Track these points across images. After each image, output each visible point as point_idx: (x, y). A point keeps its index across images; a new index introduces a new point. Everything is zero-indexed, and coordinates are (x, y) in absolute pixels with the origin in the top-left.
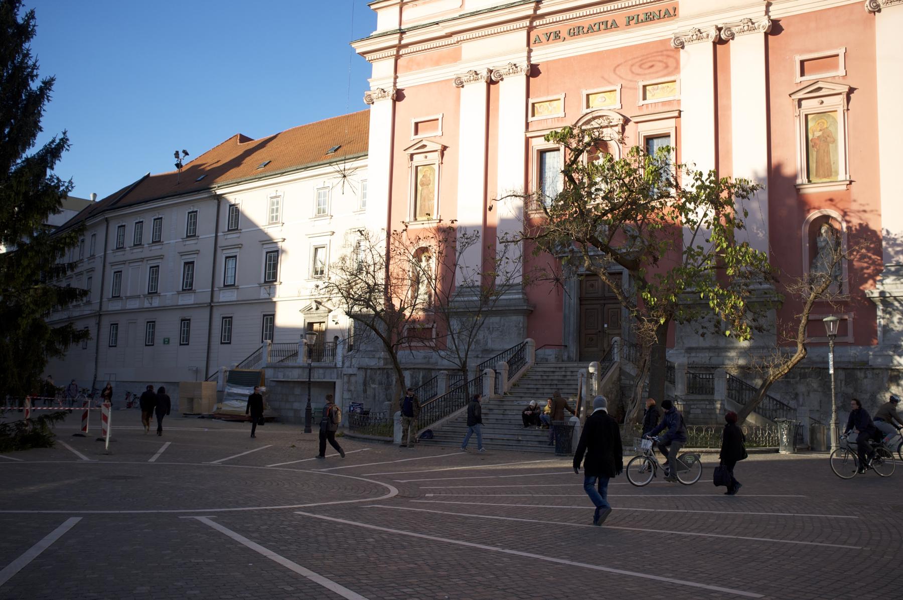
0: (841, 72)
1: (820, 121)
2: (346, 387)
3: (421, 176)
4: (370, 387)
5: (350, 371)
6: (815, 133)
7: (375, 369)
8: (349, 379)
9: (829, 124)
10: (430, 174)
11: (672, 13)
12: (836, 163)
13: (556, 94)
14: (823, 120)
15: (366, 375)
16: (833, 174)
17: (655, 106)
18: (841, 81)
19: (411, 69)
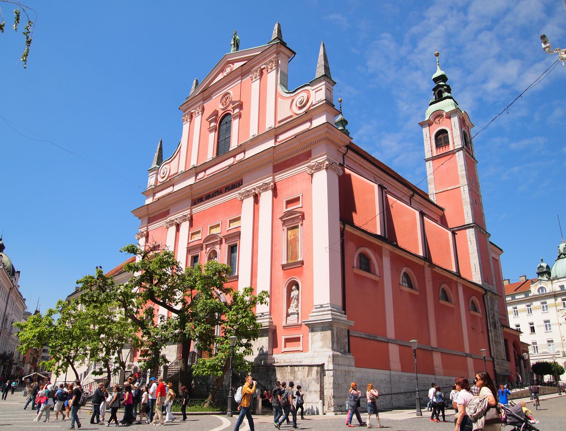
11: (241, 184)
12: (298, 252)
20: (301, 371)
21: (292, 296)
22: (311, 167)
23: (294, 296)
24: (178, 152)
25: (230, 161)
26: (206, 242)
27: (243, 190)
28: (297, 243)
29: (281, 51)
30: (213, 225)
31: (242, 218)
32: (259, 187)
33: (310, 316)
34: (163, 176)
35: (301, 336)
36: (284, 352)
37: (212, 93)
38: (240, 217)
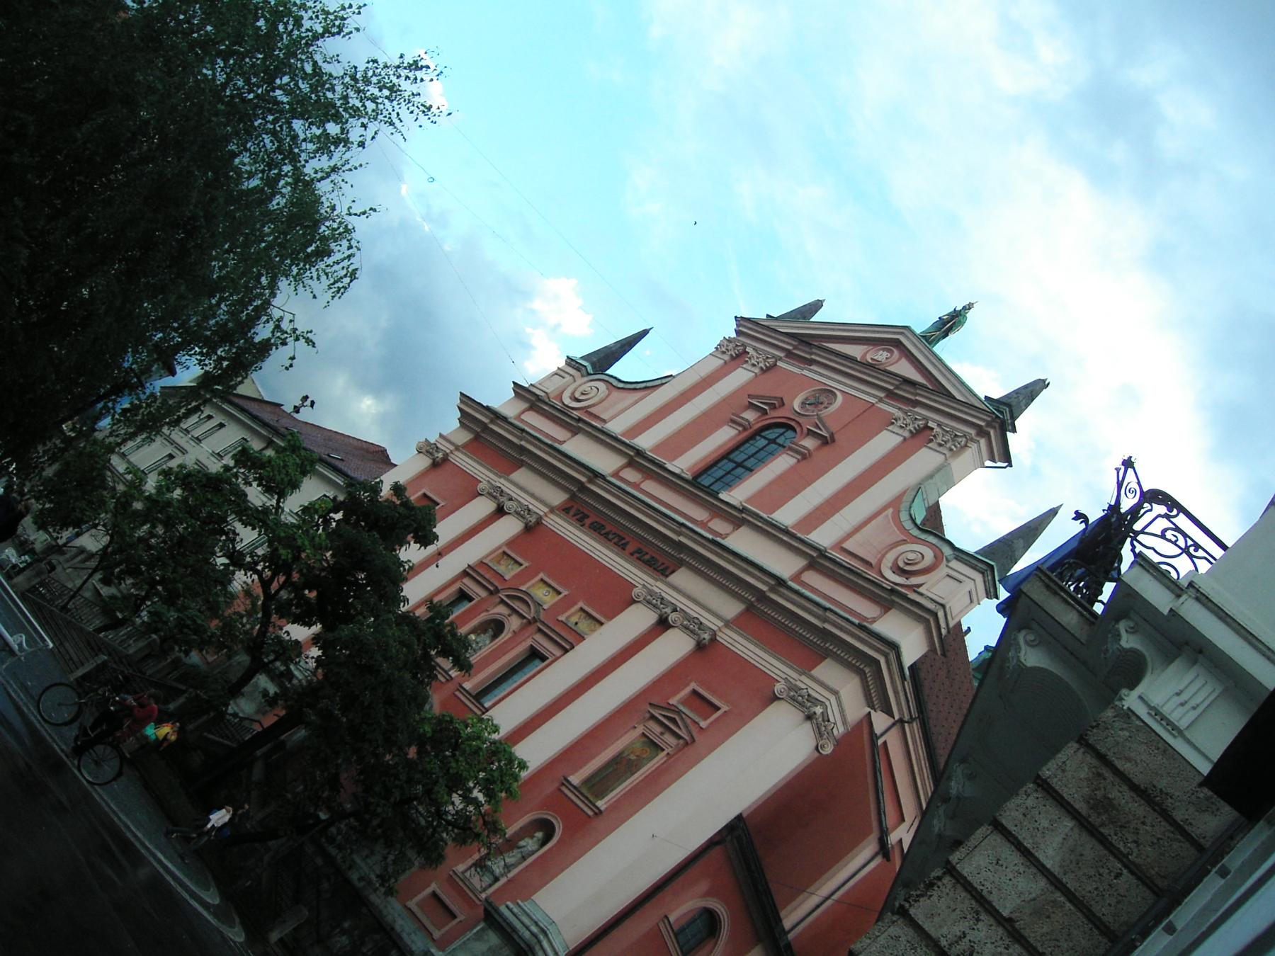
11: (667, 573)
13: (526, 559)
14: (648, 750)
21: (522, 843)
22: (792, 688)
23: (524, 847)
24: (646, 388)
25: (699, 514)
26: (507, 596)
27: (659, 587)
29: (987, 435)
31: (604, 626)
33: (507, 907)
34: (577, 395)
35: (461, 917)
36: (410, 909)
37: (812, 362)
38: (602, 624)
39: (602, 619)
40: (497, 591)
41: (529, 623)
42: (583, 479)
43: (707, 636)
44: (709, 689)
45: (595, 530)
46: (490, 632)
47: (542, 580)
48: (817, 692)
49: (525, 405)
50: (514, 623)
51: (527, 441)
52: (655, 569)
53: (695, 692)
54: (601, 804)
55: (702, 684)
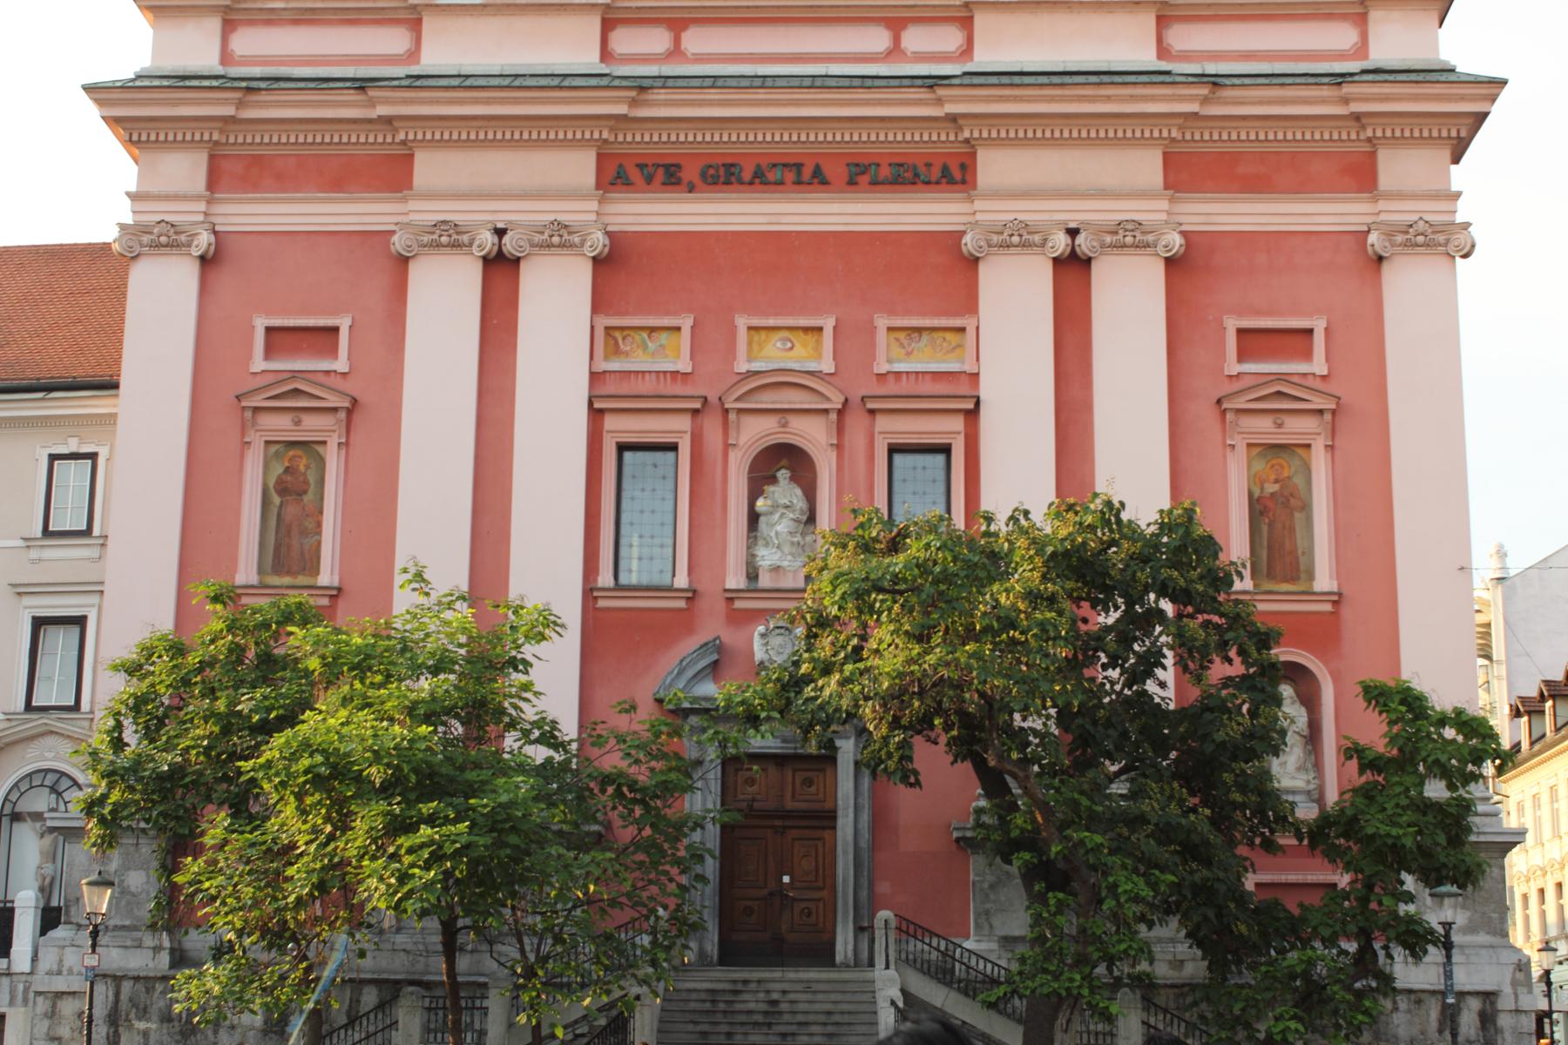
0: (1318, 365)
1: (1274, 462)
2: (43, 1027)
3: (280, 470)
4: (131, 1027)
5: (60, 984)
6: (1266, 485)
7: (146, 978)
8: (54, 1006)
9: (1293, 470)
10: (307, 467)
11: (957, 174)
13: (676, 313)
14: (1280, 461)
15: (117, 994)
16: (1303, 576)
17: (917, 379)
18: (1318, 384)
19: (256, 187)
20: (1409, 1011)
22: (1390, 232)
26: (737, 400)
28: (1297, 515)
30: (771, 322)
32: (1100, 230)
39: (958, 322)
40: (706, 398)
41: (840, 412)
42: (622, 109)
43: (1176, 241)
44: (1258, 313)
45: (727, 183)
46: (783, 475)
47: (750, 328)
48: (1432, 211)
49: (214, 25)
50: (813, 435)
51: (387, 101)
52: (929, 183)
53: (1241, 332)
54: (1324, 581)
55: (1240, 312)
